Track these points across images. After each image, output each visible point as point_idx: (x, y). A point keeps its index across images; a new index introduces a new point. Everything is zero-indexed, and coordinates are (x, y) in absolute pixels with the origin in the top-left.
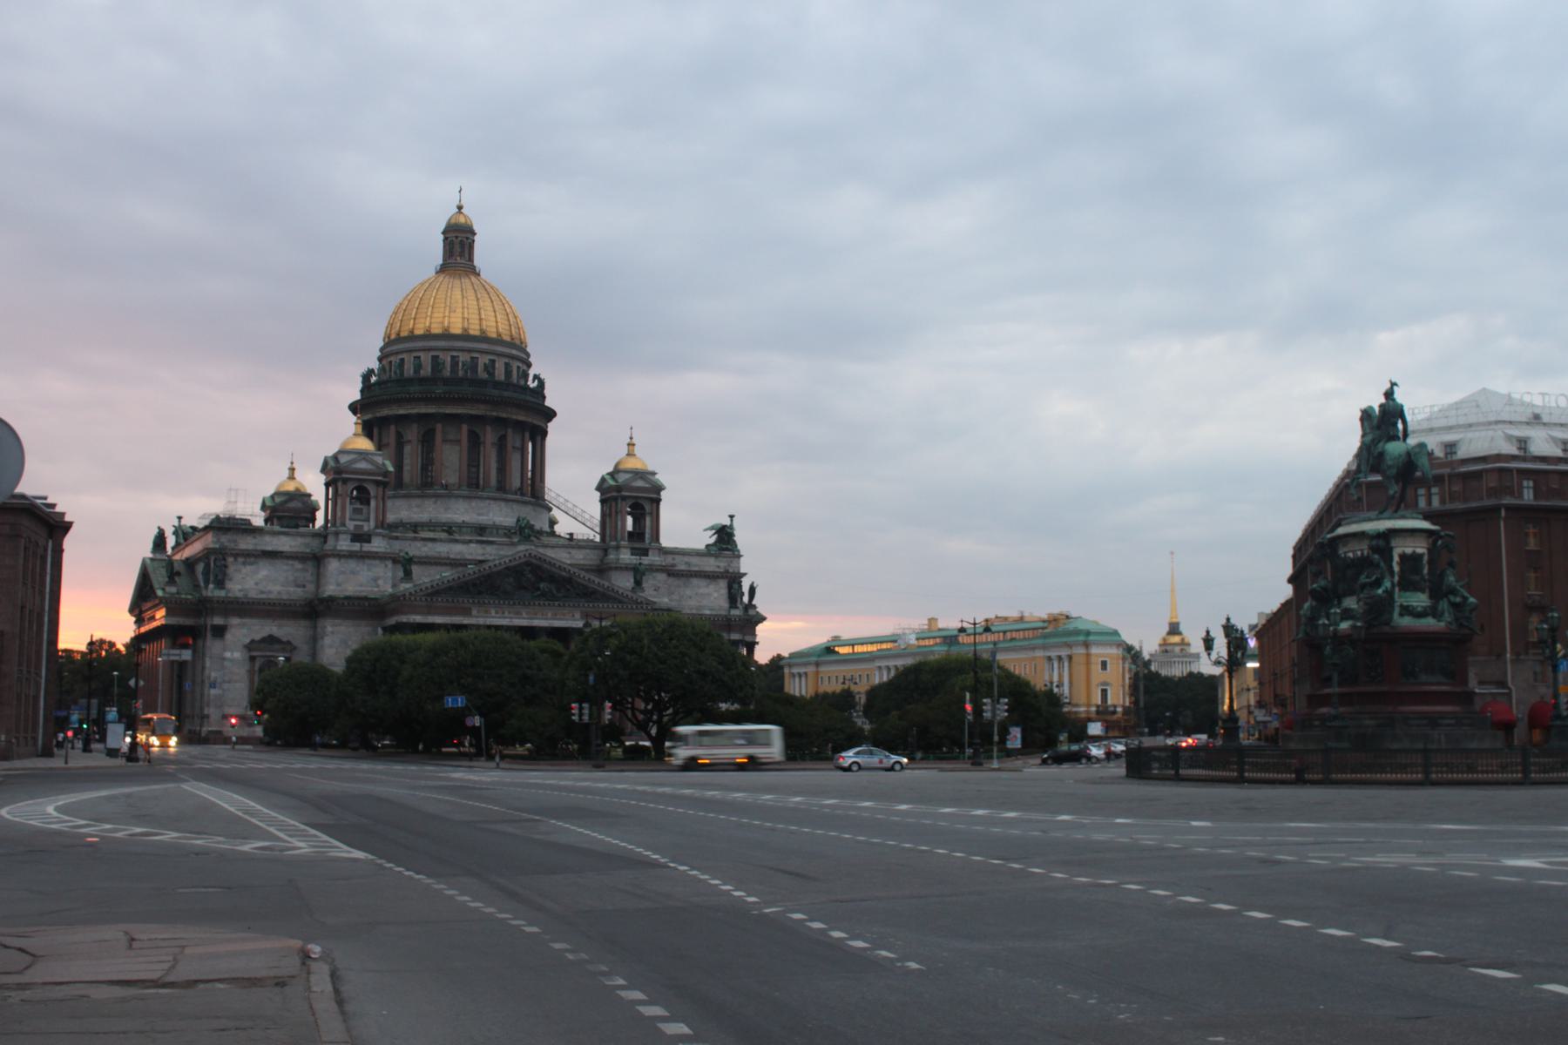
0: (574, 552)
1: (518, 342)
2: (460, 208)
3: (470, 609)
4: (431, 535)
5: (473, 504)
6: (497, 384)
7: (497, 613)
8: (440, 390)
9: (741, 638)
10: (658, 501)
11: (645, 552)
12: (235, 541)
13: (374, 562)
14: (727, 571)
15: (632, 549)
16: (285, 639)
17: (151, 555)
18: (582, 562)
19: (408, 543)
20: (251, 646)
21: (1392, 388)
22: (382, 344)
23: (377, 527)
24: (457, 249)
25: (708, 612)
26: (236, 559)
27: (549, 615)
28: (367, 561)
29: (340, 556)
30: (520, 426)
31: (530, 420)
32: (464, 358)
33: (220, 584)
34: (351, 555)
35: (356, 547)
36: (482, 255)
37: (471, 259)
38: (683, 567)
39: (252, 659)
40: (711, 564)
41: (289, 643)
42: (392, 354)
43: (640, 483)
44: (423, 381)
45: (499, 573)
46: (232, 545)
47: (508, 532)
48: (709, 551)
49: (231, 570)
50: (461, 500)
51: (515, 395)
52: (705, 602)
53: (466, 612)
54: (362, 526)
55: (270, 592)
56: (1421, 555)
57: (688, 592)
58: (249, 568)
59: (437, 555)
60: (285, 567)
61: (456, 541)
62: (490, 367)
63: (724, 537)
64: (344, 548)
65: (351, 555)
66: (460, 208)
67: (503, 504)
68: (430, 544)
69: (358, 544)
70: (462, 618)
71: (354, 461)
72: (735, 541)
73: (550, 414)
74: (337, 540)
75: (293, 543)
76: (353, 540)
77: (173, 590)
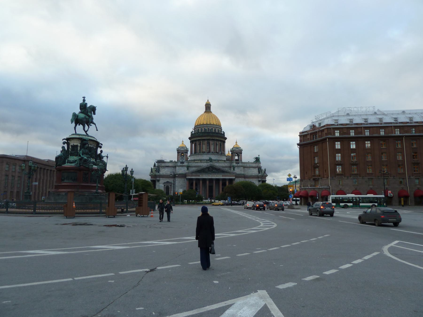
0: (225, 164)
1: (219, 125)
2: (208, 100)
3: (200, 175)
4: (197, 162)
5: (208, 156)
6: (217, 133)
7: (205, 176)
8: (201, 135)
9: (261, 179)
10: (241, 153)
11: (239, 163)
12: (161, 164)
13: (184, 167)
14: (258, 166)
15: (236, 163)
16: (170, 182)
17: (153, 168)
18: (227, 166)
19: (192, 163)
20: (164, 183)
21: (84, 99)
22: (194, 126)
23: (185, 161)
24: (207, 108)
25: (254, 175)
26: (161, 168)
27: (216, 176)
28: (183, 167)
29: (178, 166)
30: (221, 141)
31: (219, 139)
32: (211, 128)
33: (159, 172)
34: (180, 166)
35: (181, 164)
36: (212, 109)
37: (210, 110)
38: (248, 166)
39: (164, 185)
40: (254, 165)
41: (171, 182)
42: (196, 128)
43: (237, 150)
44: (203, 133)
45: (205, 168)
46: (161, 165)
47: (207, 160)
48: (254, 163)
49: (160, 170)
50: (205, 155)
51: (216, 135)
52: (253, 173)
53: (199, 176)
54: (183, 161)
55: (167, 173)
56: (77, 146)
57: (250, 171)
58: (164, 169)
59: (198, 165)
60: (170, 169)
61: (202, 163)
62: (215, 130)
63: (257, 160)
64: (179, 165)
65: (180, 166)
66: (208, 100)
67: (214, 155)
68: (197, 163)
69: (182, 164)
70: (198, 177)
71: (181, 149)
72: (259, 160)
73: (226, 139)
74: (178, 163)
75: (172, 164)
76: (181, 163)
77: (152, 173)
